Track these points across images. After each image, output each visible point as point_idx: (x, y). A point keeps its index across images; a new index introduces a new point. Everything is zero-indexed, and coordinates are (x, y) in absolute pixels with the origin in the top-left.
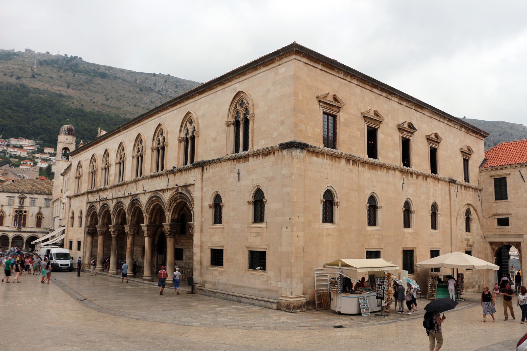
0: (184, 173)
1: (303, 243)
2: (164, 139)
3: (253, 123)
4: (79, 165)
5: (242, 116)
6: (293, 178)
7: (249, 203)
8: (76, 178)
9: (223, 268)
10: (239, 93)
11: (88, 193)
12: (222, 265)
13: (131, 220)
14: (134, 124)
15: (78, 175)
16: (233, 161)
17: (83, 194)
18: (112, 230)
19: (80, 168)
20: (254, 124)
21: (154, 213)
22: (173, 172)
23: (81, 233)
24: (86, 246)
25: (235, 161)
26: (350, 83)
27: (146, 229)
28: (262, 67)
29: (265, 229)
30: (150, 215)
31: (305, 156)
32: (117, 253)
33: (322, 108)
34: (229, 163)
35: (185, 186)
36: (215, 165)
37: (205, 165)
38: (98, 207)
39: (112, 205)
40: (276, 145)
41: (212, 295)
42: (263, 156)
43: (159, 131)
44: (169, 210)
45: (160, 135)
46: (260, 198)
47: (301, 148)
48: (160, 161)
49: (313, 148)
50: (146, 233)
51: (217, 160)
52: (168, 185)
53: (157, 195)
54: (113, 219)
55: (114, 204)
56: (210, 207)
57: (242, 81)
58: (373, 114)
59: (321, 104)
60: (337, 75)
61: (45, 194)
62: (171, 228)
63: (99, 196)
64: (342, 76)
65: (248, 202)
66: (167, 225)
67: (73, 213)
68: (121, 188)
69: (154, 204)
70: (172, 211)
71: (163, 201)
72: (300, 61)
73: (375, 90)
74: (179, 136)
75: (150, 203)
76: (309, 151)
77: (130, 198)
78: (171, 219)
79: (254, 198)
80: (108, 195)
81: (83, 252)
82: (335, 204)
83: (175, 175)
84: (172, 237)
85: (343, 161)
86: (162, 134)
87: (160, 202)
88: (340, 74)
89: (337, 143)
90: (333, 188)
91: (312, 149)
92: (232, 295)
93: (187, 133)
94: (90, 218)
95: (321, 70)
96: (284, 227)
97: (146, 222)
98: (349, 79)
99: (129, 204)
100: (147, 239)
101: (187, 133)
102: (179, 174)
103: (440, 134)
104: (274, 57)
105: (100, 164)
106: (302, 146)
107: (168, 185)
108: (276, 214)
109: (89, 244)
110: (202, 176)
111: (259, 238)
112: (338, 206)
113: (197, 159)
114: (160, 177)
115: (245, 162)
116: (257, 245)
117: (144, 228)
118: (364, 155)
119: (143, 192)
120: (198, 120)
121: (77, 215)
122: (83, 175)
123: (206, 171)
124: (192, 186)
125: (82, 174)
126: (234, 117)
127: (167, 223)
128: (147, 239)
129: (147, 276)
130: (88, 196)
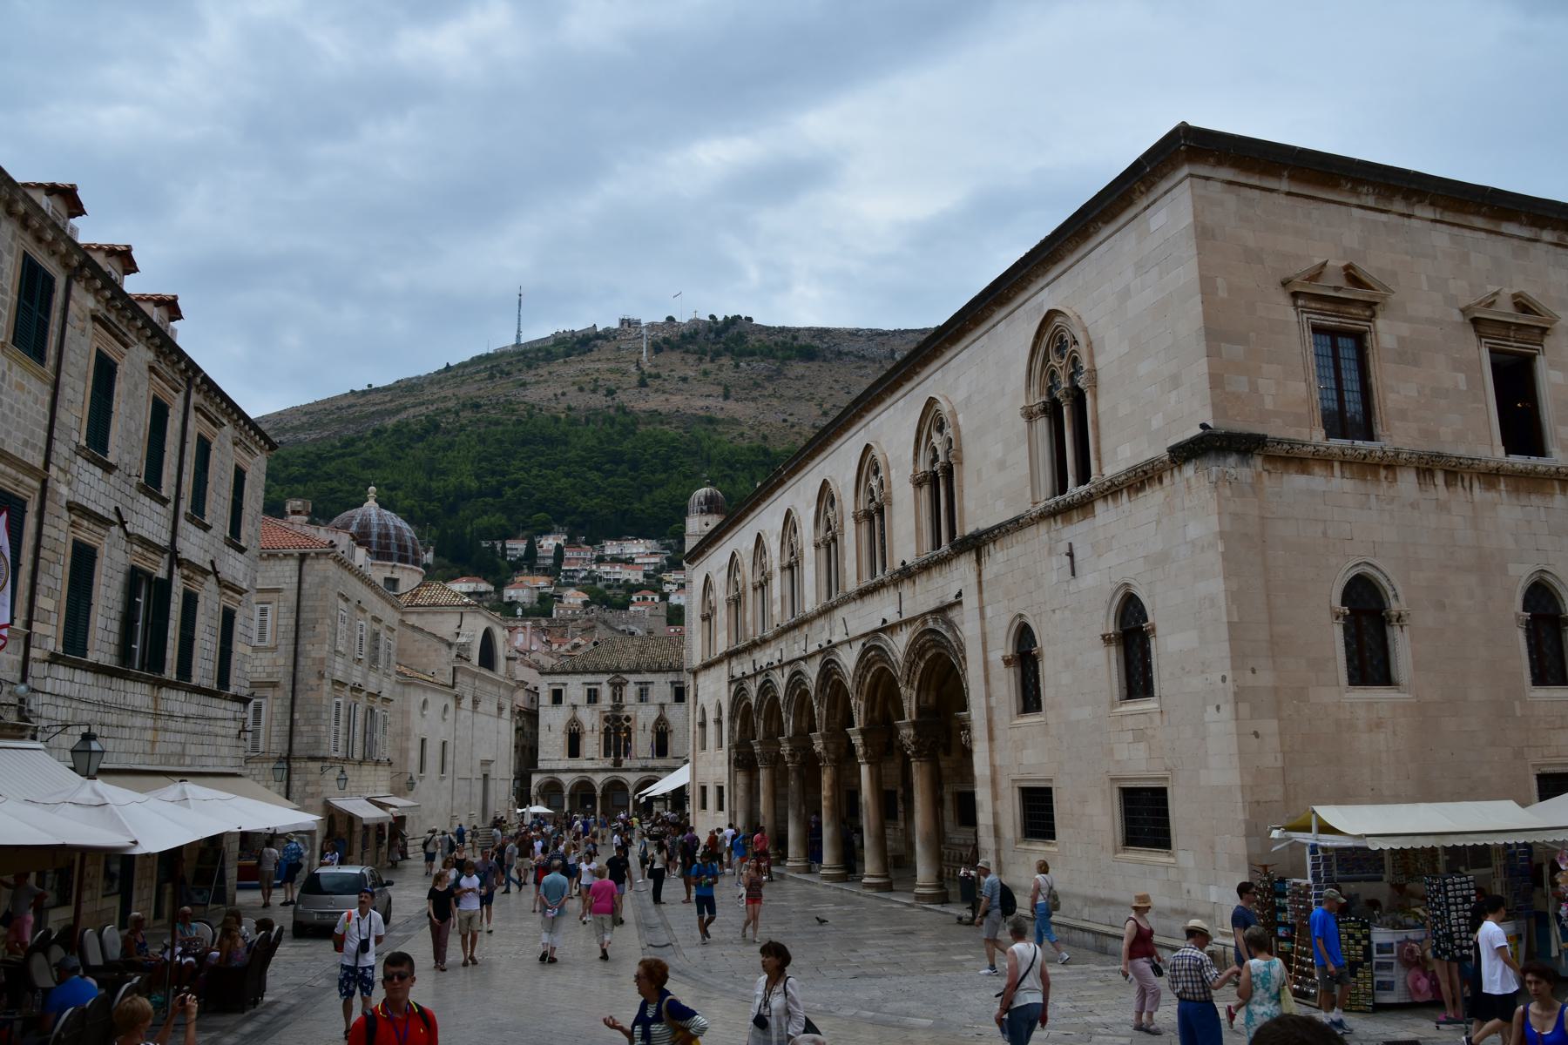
0: (935, 572)
1: (1279, 756)
2: (881, 485)
3: (1095, 397)
4: (707, 583)
7: (1106, 639)
8: (704, 619)
9: (1054, 845)
10: (1052, 314)
11: (730, 655)
12: (1053, 836)
13: (827, 719)
14: (811, 457)
15: (707, 611)
16: (1052, 520)
18: (786, 749)
20: (1099, 401)
21: (879, 695)
22: (907, 574)
23: (722, 764)
25: (1059, 518)
26: (1406, 220)
27: (861, 741)
28: (1100, 224)
29: (1157, 718)
30: (867, 701)
31: (1259, 475)
32: (803, 811)
33: (1305, 315)
34: (1043, 527)
35: (942, 611)
36: (1008, 540)
37: (985, 544)
38: (753, 689)
39: (781, 680)
42: (1132, 491)
43: (869, 465)
44: (908, 682)
45: (871, 474)
46: (1137, 622)
47: (1238, 452)
48: (877, 544)
49: (1286, 447)
50: (861, 751)
51: (1010, 522)
52: (900, 613)
53: (878, 644)
54: (788, 720)
55: (785, 680)
56: (1007, 662)
57: (1054, 280)
58: (1509, 308)
59: (1300, 302)
60: (1354, 201)
61: (671, 669)
62: (917, 734)
63: (754, 661)
64: (1370, 201)
65: (1103, 637)
66: (907, 725)
67: (703, 710)
68: (796, 633)
69: (873, 670)
70: (916, 683)
71: (893, 659)
72: (1207, 179)
73: (1510, 228)
74: (915, 471)
75: (863, 668)
76: (1270, 458)
77: (818, 659)
78: (918, 708)
79: (1121, 626)
80: (772, 655)
81: (730, 816)
82: (1390, 621)
83: (914, 583)
85: (1407, 481)
86: (876, 472)
87: (887, 663)
88: (1363, 197)
89: (1378, 420)
90: (1378, 569)
91: (1280, 451)
92: (1083, 930)
93: (935, 459)
95: (1289, 194)
96: (1208, 708)
97: (859, 721)
98: (1399, 206)
99: (819, 676)
100: (865, 770)
101: (935, 459)
102: (924, 577)
103: (1532, 292)
104: (1127, 186)
105: (747, 575)
106: (1243, 445)
107: (900, 613)
108: (1183, 669)
109: (741, 793)
110: (980, 575)
111: (1142, 745)
112: (1405, 628)
113: (968, 526)
114: (881, 591)
115: (1085, 518)
116: (1140, 768)
117: (857, 740)
118: (1494, 451)
119: (846, 638)
120: (954, 415)
121: (711, 716)
123: (987, 558)
124: (958, 608)
125: (715, 608)
127: (908, 720)
128: (865, 770)
129: (872, 876)
130: (730, 664)
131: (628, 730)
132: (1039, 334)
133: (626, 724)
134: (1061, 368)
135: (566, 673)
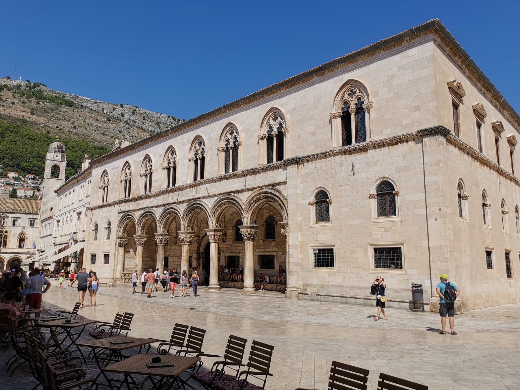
5: (353, 106)
6: (441, 165)
11: (121, 202)
15: (102, 184)
17: (113, 204)
19: (105, 177)
21: (220, 217)
24: (118, 258)
30: (216, 219)
40: (414, 130)
41: (321, 299)
63: (138, 204)
81: (114, 265)
84: (251, 240)
94: (122, 228)
111: (389, 233)
122: (111, 184)
126: (340, 109)
129: (215, 285)
131: (6, 237)
132: (341, 89)
133: (5, 234)
134: (351, 101)
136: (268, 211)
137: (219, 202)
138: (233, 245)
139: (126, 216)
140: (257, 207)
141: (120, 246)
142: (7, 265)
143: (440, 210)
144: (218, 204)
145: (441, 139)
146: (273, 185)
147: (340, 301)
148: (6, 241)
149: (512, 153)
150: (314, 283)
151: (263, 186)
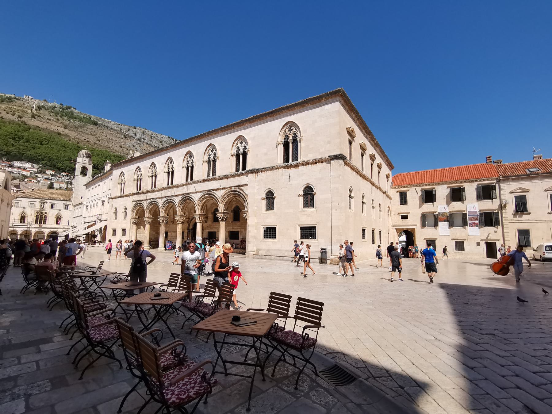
5: (291, 138)
6: (341, 178)
12: (275, 238)
15: (120, 182)
17: (128, 196)
19: (122, 177)
40: (326, 156)
45: (210, 151)
70: (224, 203)
81: (130, 237)
108: (325, 202)
131: (45, 217)
132: (284, 126)
133: (45, 214)
135: (22, 197)
136: (235, 203)
137: (203, 196)
138: (212, 224)
139: (138, 205)
140: (228, 200)
141: (134, 224)
142: (47, 236)
143: (339, 204)
144: (203, 198)
145: (341, 162)
146: (239, 186)
147: (279, 259)
148: (46, 219)
149: (379, 172)
150: (264, 248)
151: (232, 187)
